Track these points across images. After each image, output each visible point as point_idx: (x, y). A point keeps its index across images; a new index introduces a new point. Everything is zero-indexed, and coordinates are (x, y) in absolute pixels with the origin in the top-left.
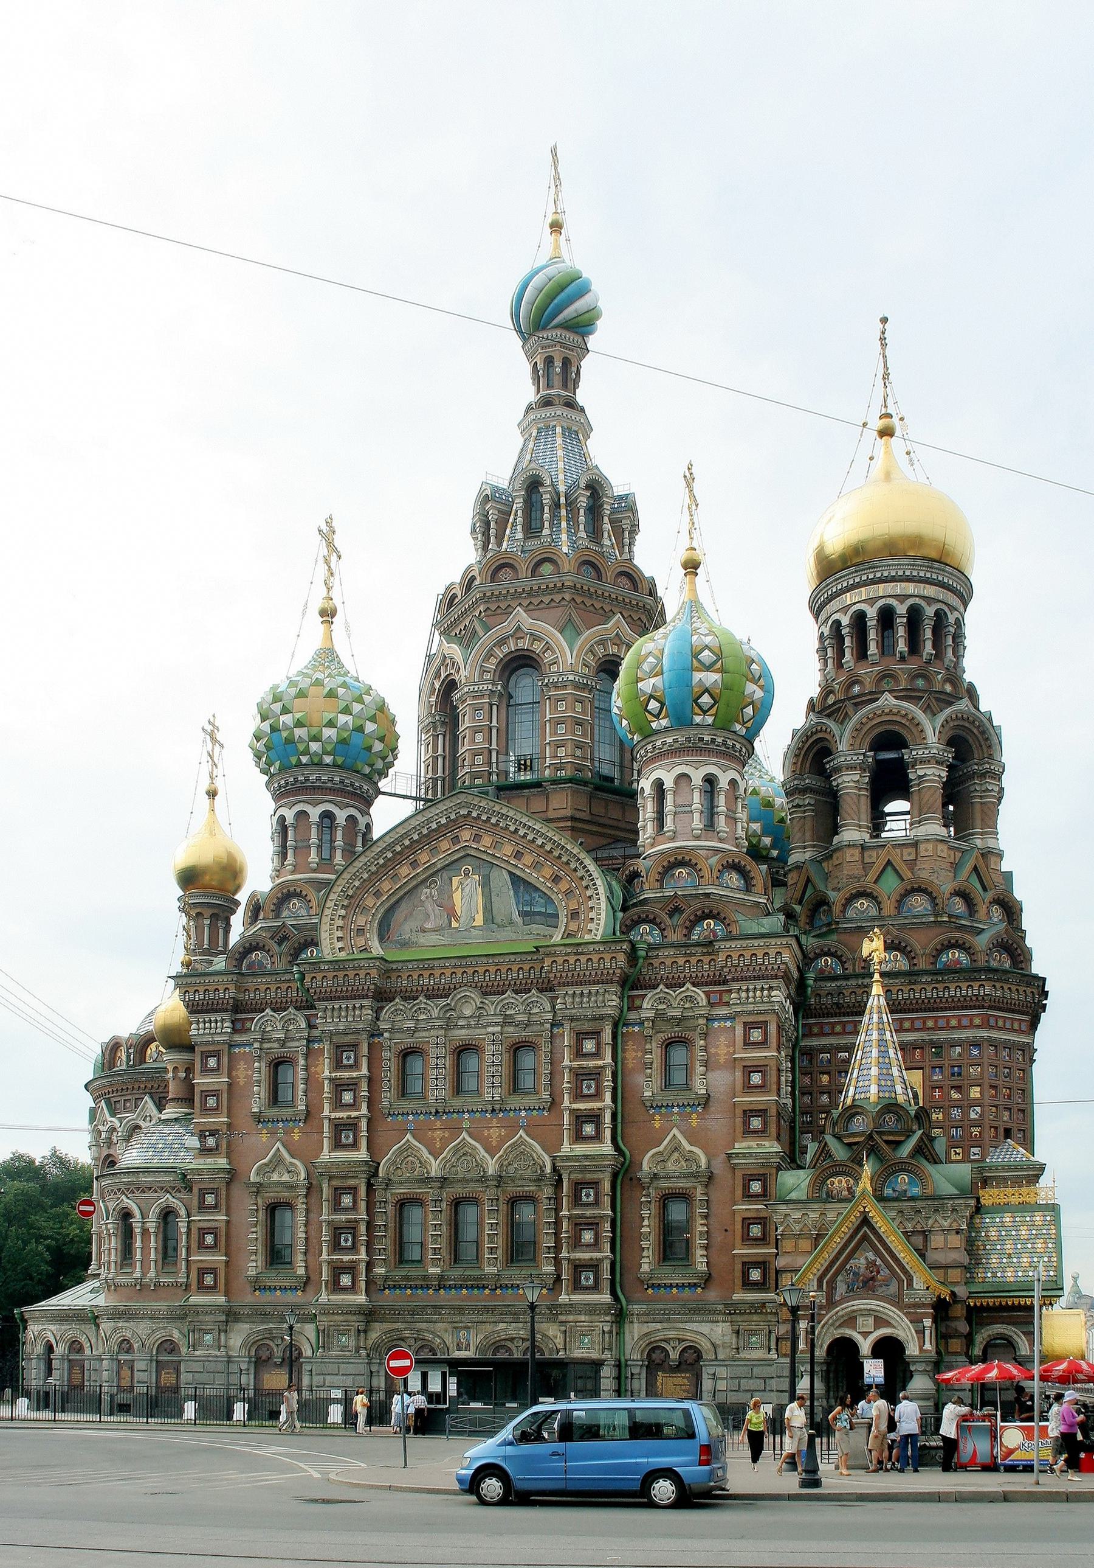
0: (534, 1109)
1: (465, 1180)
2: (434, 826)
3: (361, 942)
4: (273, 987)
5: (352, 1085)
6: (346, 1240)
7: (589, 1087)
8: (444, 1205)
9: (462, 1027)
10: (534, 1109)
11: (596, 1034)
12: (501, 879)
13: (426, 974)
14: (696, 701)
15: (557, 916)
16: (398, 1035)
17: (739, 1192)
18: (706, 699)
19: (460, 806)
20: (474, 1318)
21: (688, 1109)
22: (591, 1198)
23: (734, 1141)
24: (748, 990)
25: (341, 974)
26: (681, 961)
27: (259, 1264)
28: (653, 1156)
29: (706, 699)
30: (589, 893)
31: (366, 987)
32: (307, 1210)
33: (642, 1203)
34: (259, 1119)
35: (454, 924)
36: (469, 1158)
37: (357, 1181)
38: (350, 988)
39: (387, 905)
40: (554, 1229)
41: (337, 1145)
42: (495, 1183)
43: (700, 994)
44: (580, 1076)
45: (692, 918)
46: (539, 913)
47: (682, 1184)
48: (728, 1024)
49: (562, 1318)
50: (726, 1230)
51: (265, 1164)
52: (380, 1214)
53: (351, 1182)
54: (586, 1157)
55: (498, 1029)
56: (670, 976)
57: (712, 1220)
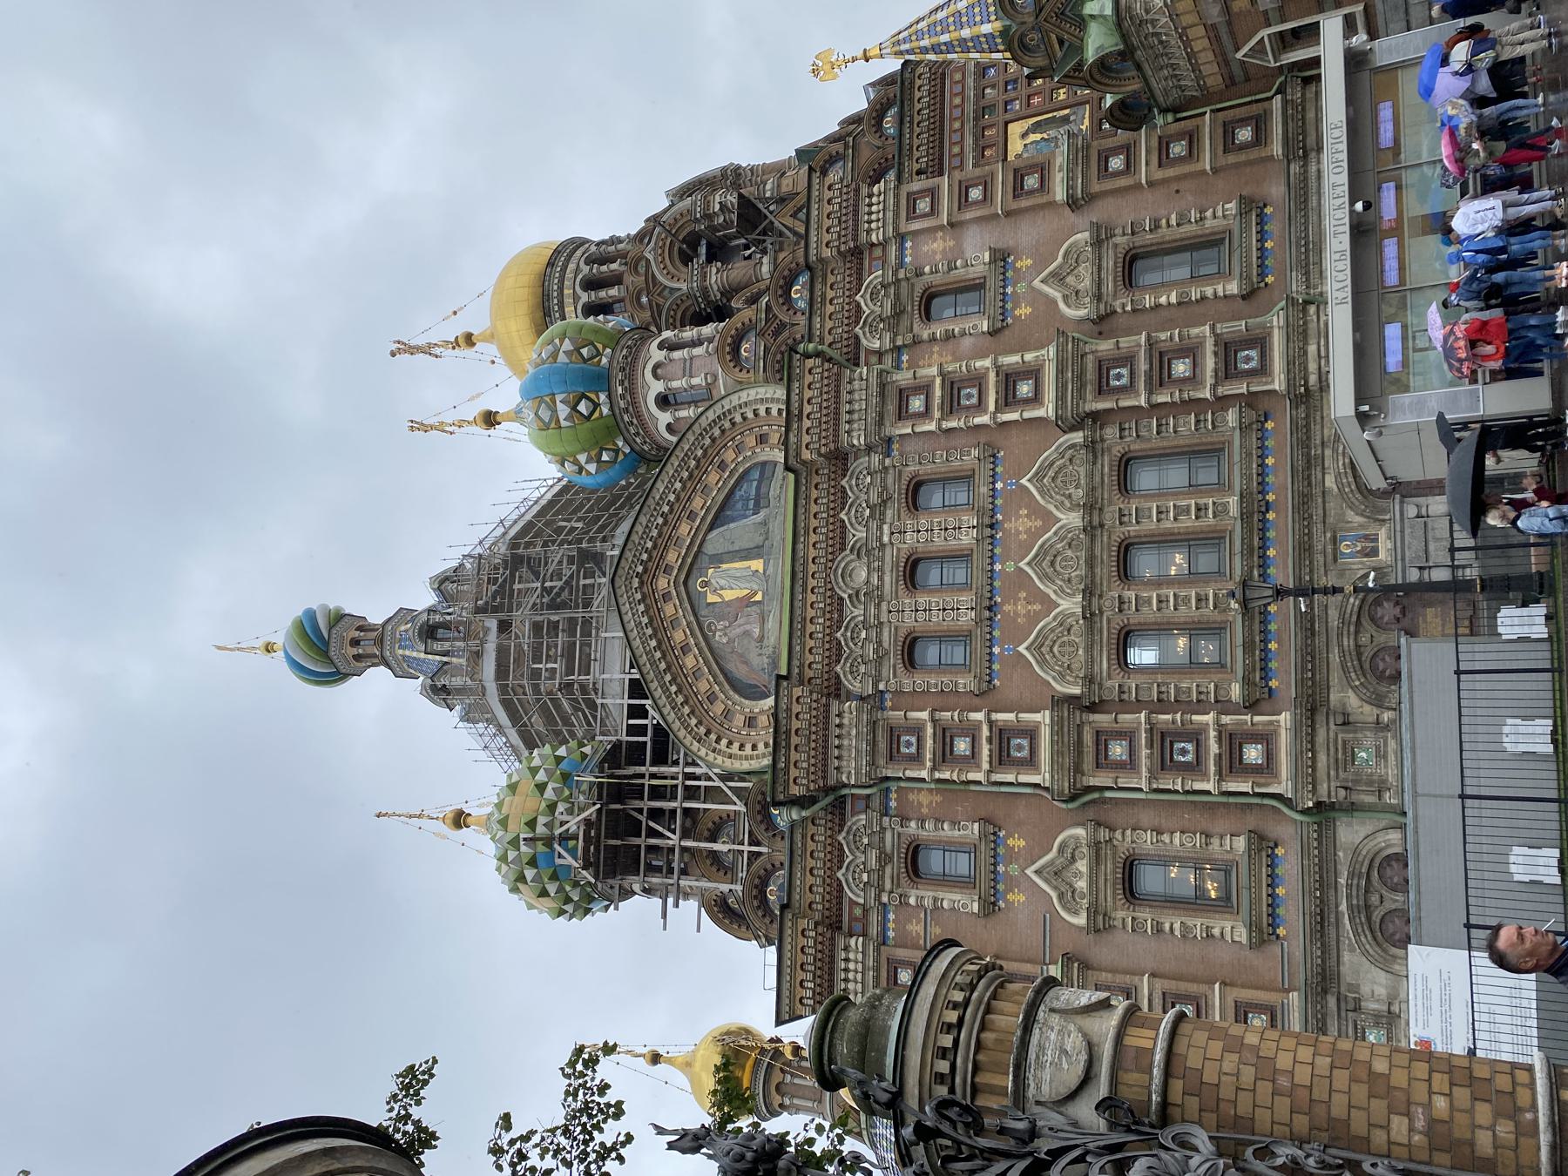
0: (993, 470)
1: (1091, 562)
2: (645, 620)
3: (763, 720)
4: (811, 863)
5: (945, 737)
6: (1184, 752)
7: (969, 395)
8: (1130, 595)
9: (881, 578)
10: (993, 470)
11: (903, 395)
12: (716, 541)
13: (810, 628)
14: (585, 361)
15: (764, 464)
16: (885, 673)
17: (1123, 182)
18: (585, 351)
19: (628, 588)
20: (1317, 529)
21: (1009, 274)
22: (1124, 371)
23: (1052, 204)
24: (870, 222)
25: (795, 740)
26: (830, 309)
27: (1228, 925)
28: (1069, 307)
29: (585, 351)
30: (738, 419)
31: (814, 705)
32: (1134, 829)
33: (1134, 310)
34: (990, 907)
35: (758, 597)
36: (1059, 558)
37: (1086, 728)
38: (814, 729)
39: (727, 686)
40: (1167, 417)
41: (1031, 762)
42: (1096, 513)
43: (874, 277)
44: (952, 405)
45: (785, 308)
46: (758, 488)
47: (1109, 263)
48: (908, 244)
49: (1313, 379)
50: (1177, 191)
51: (1061, 896)
52: (1141, 692)
53: (1088, 738)
54: (1060, 371)
55: (886, 527)
56: (846, 321)
57: (1163, 212)
